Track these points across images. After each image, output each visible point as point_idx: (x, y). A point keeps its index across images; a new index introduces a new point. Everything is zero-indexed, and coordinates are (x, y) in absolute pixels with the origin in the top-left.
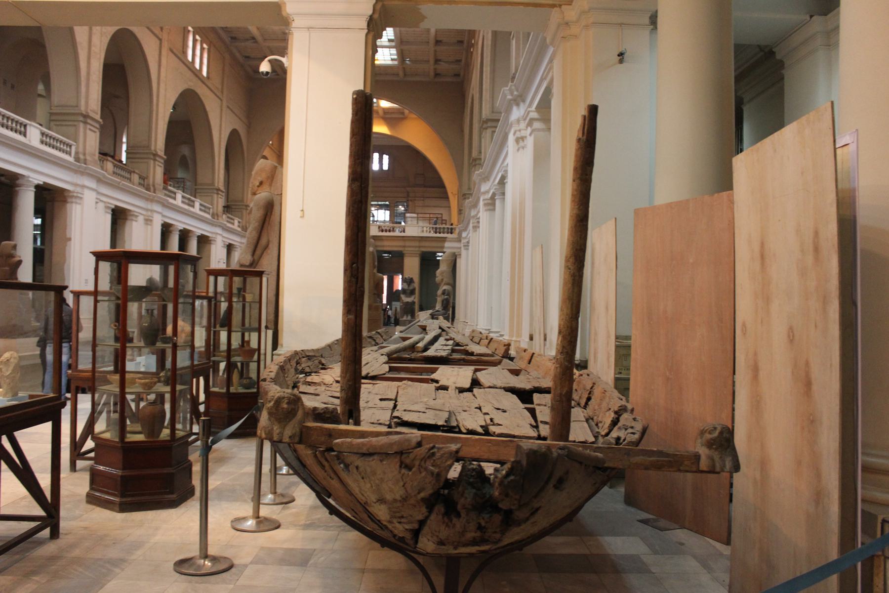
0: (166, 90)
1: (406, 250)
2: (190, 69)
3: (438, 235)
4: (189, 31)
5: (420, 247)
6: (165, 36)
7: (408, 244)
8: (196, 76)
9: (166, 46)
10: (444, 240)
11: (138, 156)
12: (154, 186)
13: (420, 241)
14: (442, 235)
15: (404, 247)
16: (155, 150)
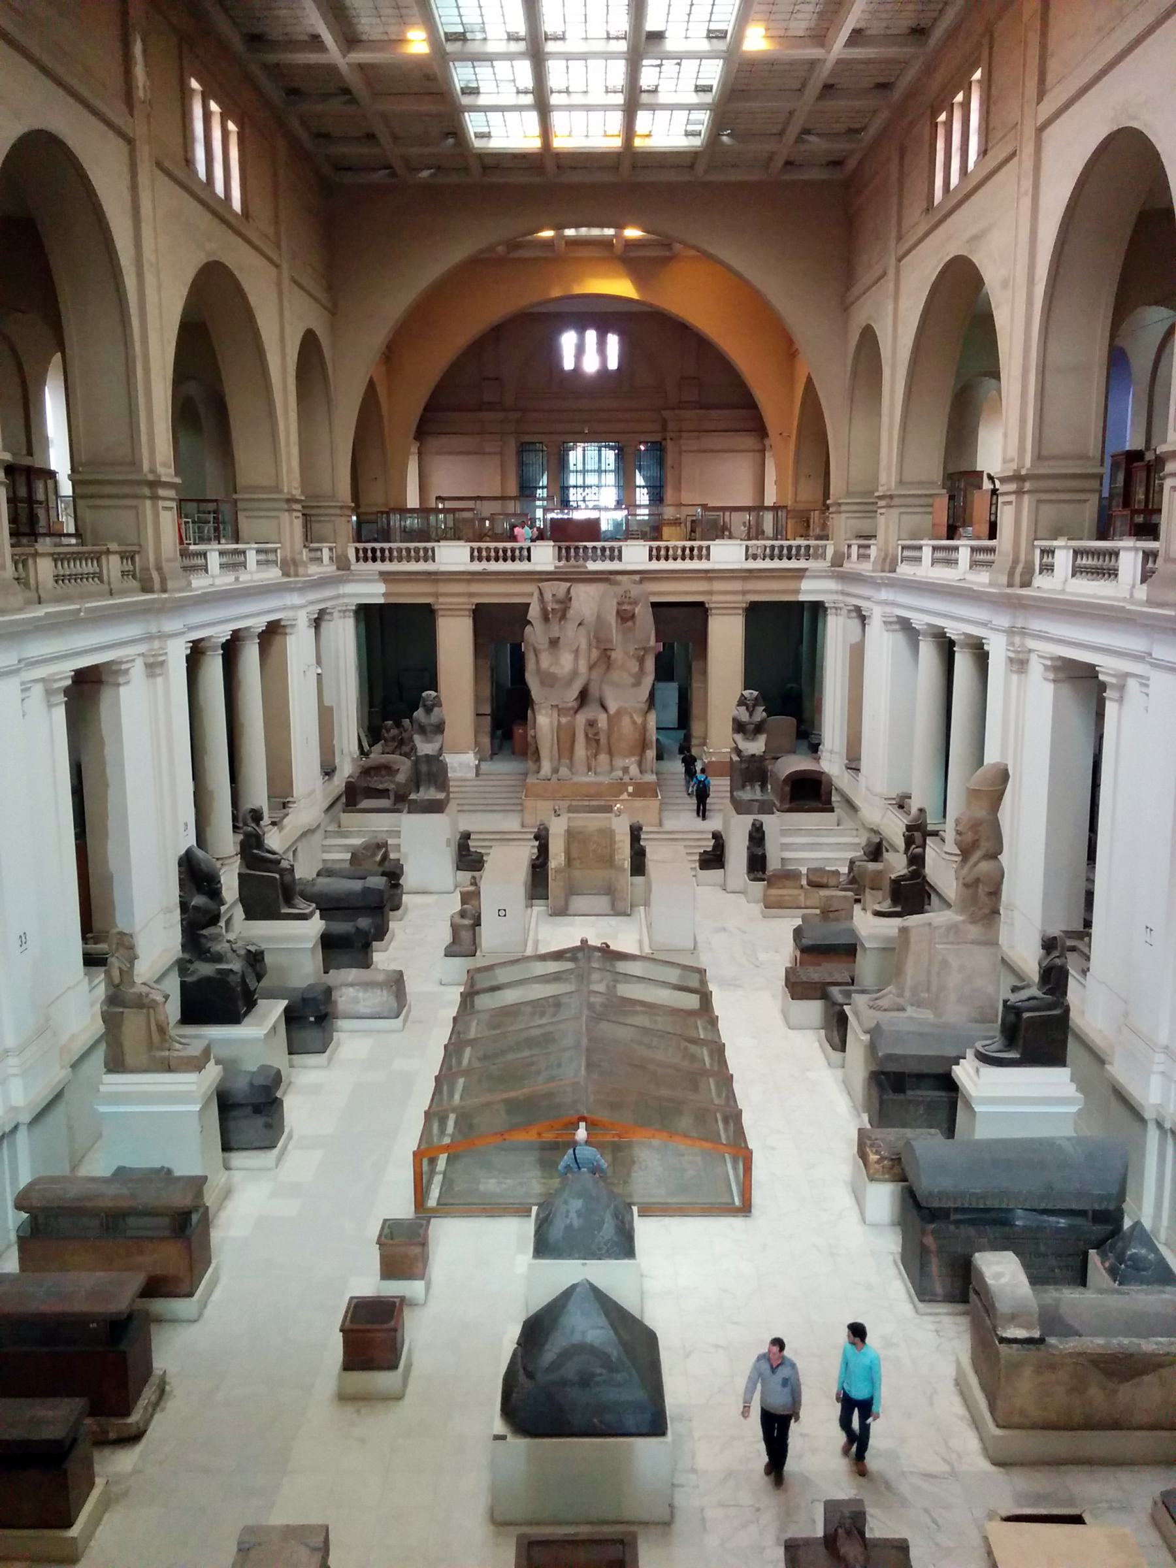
0: (159, 288)
1: (711, 601)
2: (202, 202)
3: (785, 564)
4: (193, 90)
5: (744, 593)
6: (139, 128)
7: (718, 586)
8: (215, 214)
9: (145, 153)
10: (800, 574)
11: (108, 490)
12: (159, 569)
13: (744, 579)
14: (793, 564)
15: (711, 593)
16: (153, 471)
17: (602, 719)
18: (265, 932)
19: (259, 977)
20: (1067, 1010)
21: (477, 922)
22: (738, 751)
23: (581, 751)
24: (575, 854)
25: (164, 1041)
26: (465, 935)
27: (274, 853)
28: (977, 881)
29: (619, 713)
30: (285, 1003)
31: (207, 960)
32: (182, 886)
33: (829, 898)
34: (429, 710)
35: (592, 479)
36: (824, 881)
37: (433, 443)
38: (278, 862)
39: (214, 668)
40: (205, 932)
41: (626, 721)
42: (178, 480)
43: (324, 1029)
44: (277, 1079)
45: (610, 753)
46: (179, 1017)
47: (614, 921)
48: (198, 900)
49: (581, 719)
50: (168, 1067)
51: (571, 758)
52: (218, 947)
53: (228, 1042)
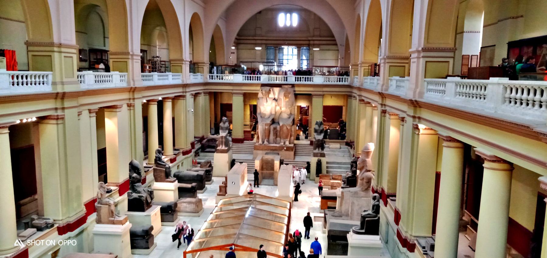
17: (278, 127)
18: (157, 185)
19: (152, 199)
20: (379, 218)
21: (226, 187)
22: (315, 138)
23: (272, 137)
24: (264, 167)
25: (113, 215)
26: (223, 189)
27: (164, 162)
28: (363, 178)
29: (283, 126)
30: (159, 207)
31: (136, 193)
32: (130, 171)
33: (333, 183)
34: (224, 123)
35: (290, 57)
36: (337, 178)
37: (241, 46)
38: (165, 165)
39: (154, 109)
40: (136, 185)
41: (285, 128)
42: (141, 54)
43: (173, 215)
44: (152, 228)
45: (280, 138)
46: (127, 209)
47: (273, 187)
48: (135, 175)
49: (272, 127)
50: (113, 223)
51: (269, 138)
52: (139, 189)
53: (140, 216)
